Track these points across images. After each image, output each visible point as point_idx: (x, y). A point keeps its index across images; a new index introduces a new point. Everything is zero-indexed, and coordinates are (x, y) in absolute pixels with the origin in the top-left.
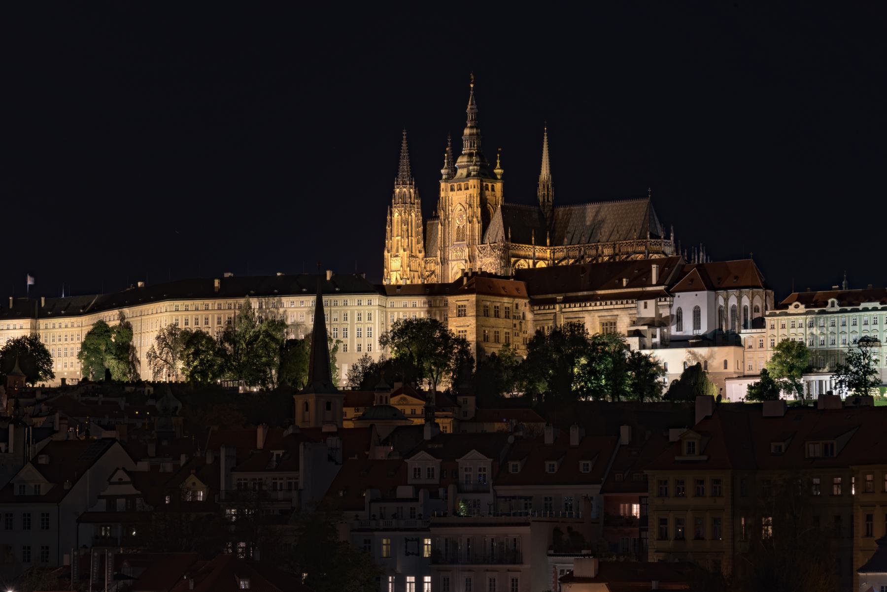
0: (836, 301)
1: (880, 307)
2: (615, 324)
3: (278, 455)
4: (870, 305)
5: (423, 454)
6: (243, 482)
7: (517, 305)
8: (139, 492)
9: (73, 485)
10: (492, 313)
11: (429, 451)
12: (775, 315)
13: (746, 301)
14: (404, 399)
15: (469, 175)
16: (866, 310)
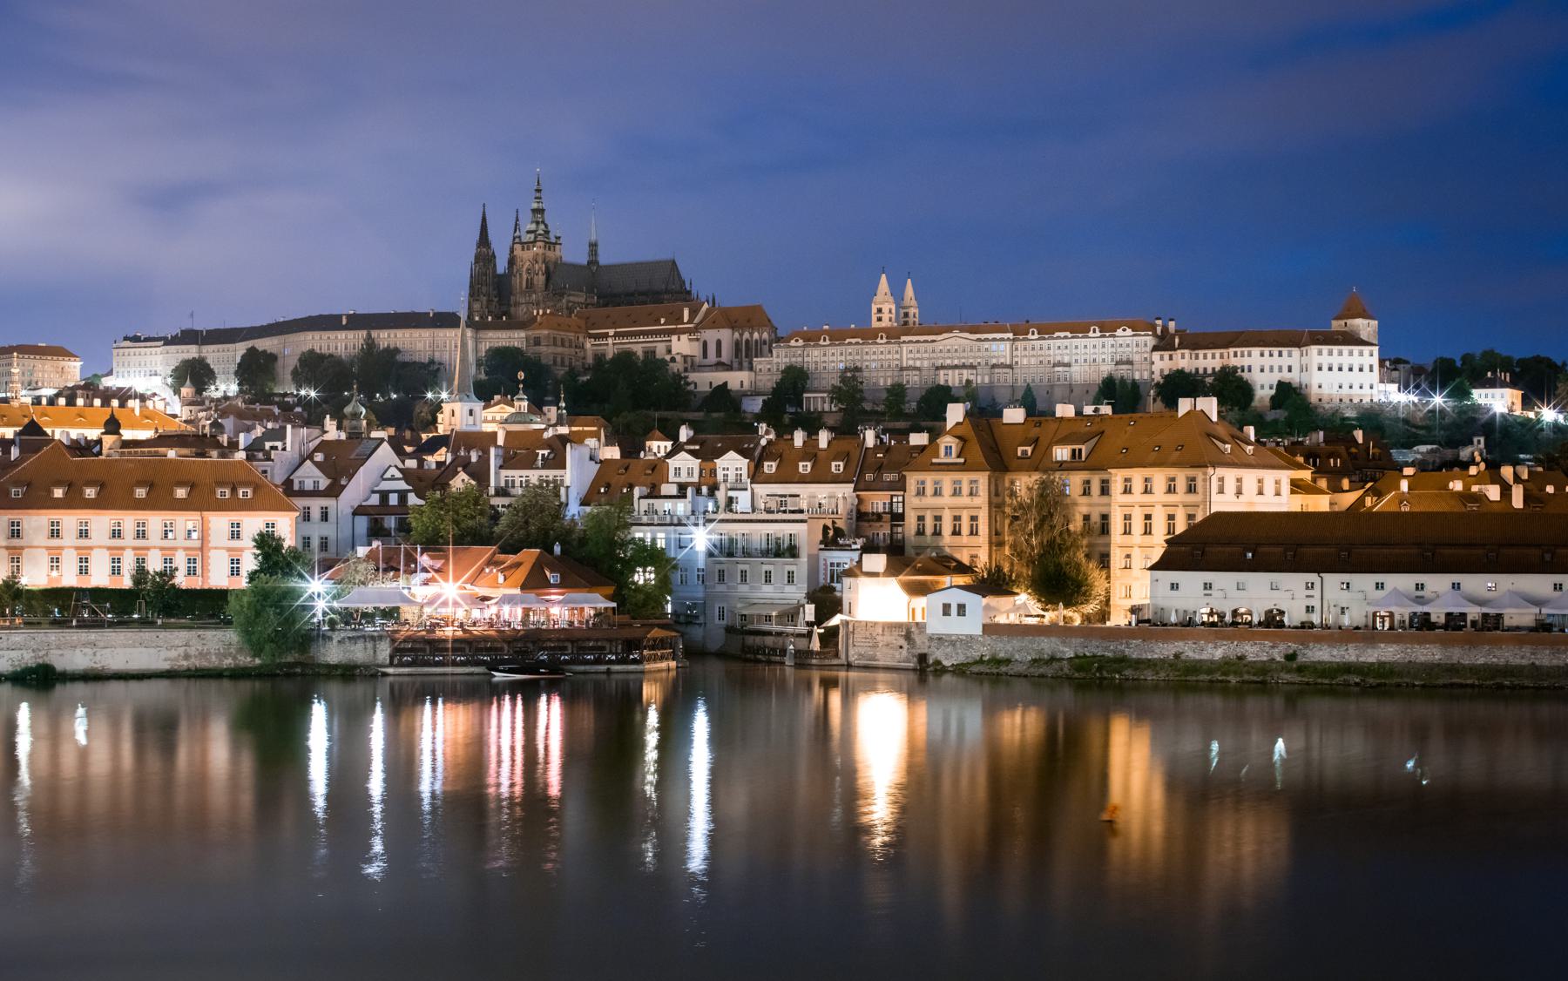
0: (827, 338)
1: (861, 341)
3: (543, 455)
4: (854, 341)
5: (683, 455)
6: (510, 479)
7: (578, 338)
8: (411, 488)
9: (349, 481)
10: (559, 343)
11: (692, 453)
12: (780, 347)
13: (756, 335)
14: (502, 408)
15: (536, 237)
16: (850, 344)
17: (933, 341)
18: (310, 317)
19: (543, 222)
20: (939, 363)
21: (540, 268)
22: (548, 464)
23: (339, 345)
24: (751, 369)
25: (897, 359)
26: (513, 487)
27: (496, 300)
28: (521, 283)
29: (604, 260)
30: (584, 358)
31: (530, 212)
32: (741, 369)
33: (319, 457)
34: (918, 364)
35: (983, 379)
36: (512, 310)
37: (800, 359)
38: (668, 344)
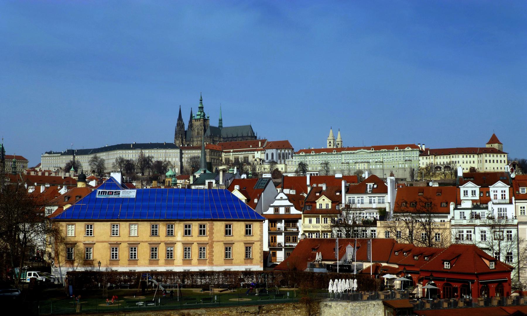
1: (326, 153)
2: (248, 157)
3: (370, 186)
4: (324, 153)
6: (352, 199)
8: (292, 204)
13: (287, 151)
15: (200, 117)
17: (354, 153)
18: (118, 145)
19: (203, 111)
20: (355, 161)
22: (374, 191)
23: (130, 155)
25: (340, 160)
26: (354, 203)
27: (184, 140)
28: (195, 133)
30: (222, 160)
31: (198, 108)
32: (281, 163)
33: (237, 187)
35: (372, 167)
37: (303, 160)
38: (253, 155)
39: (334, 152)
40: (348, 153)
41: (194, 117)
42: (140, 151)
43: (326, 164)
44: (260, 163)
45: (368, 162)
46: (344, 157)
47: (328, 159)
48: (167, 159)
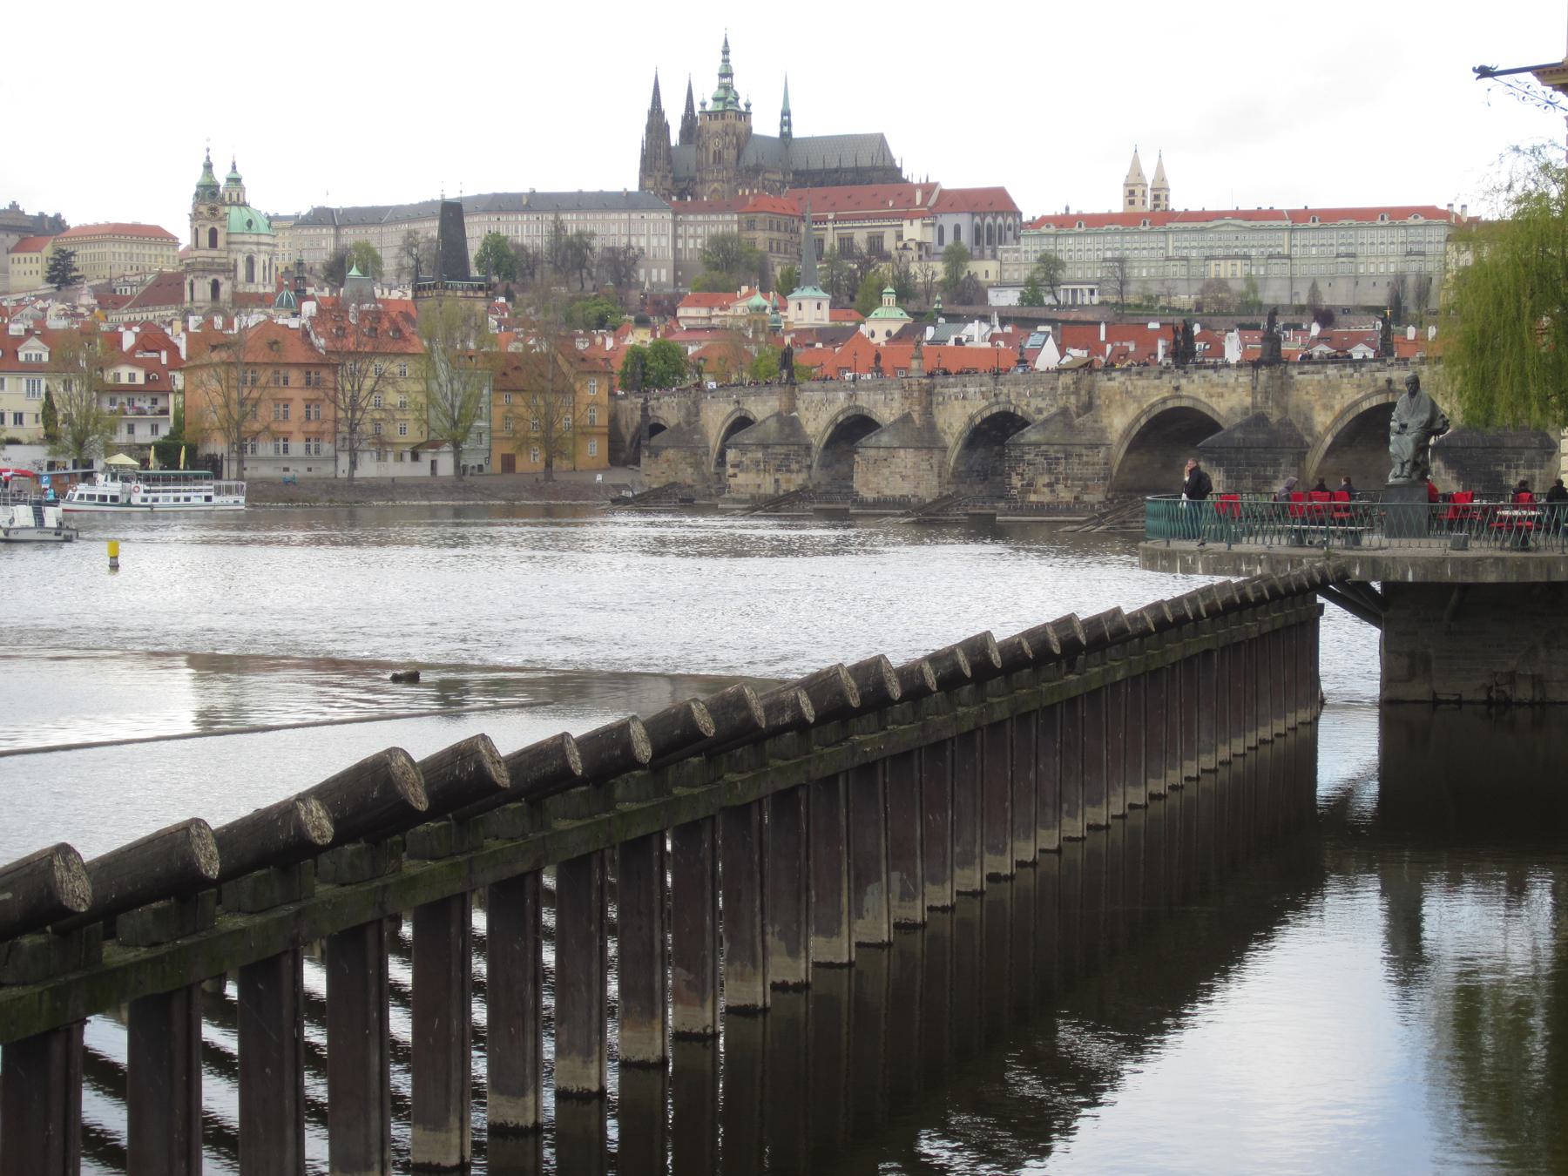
2: (881, 237)
4: (1113, 227)
15: (725, 105)
16: (1108, 233)
17: (1203, 230)
20: (1207, 252)
21: (731, 141)
24: (994, 257)
29: (797, 133)
32: (982, 257)
34: (1184, 253)
36: (698, 188)
37: (1052, 247)
39: (1145, 224)
40: (1185, 230)
41: (703, 105)
42: (551, 217)
43: (1122, 261)
44: (920, 257)
45: (1247, 257)
46: (1173, 244)
47: (1126, 246)
48: (634, 241)
